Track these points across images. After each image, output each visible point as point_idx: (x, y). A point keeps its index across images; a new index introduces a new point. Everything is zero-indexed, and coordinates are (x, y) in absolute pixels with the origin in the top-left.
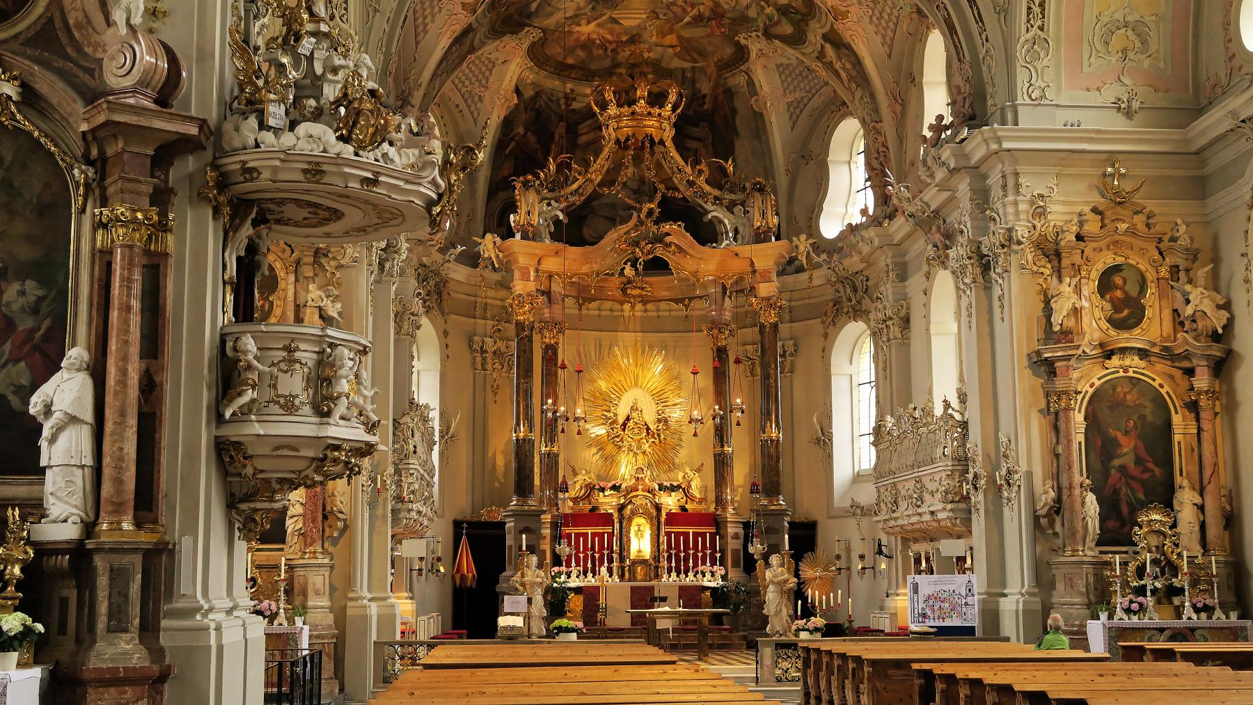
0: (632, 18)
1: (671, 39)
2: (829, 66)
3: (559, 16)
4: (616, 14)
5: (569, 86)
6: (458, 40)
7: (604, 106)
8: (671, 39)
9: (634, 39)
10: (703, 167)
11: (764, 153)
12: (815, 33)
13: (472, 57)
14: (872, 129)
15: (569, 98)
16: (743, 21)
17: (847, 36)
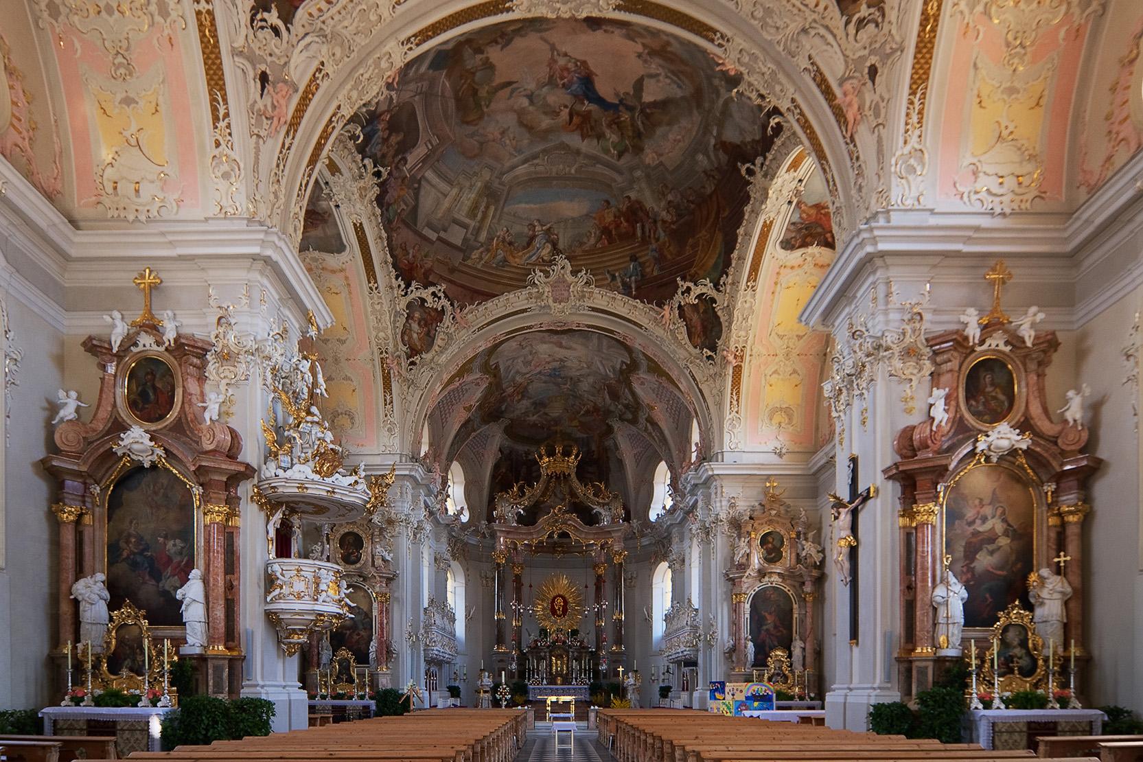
0: (556, 411)
1: (575, 423)
2: (650, 434)
3: (517, 412)
4: (547, 410)
5: (526, 448)
6: (464, 425)
7: (541, 457)
8: (575, 423)
9: (557, 421)
10: (589, 486)
11: (623, 478)
12: (642, 420)
13: (473, 434)
14: (671, 467)
15: (527, 453)
16: (608, 413)
17: (656, 419)
